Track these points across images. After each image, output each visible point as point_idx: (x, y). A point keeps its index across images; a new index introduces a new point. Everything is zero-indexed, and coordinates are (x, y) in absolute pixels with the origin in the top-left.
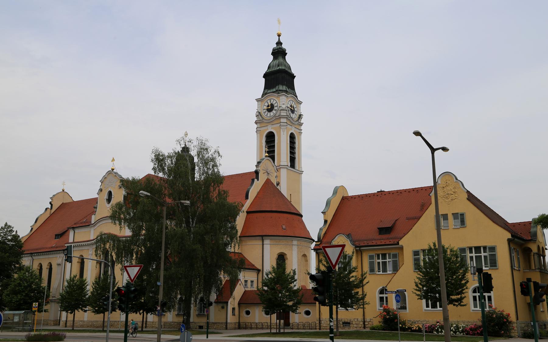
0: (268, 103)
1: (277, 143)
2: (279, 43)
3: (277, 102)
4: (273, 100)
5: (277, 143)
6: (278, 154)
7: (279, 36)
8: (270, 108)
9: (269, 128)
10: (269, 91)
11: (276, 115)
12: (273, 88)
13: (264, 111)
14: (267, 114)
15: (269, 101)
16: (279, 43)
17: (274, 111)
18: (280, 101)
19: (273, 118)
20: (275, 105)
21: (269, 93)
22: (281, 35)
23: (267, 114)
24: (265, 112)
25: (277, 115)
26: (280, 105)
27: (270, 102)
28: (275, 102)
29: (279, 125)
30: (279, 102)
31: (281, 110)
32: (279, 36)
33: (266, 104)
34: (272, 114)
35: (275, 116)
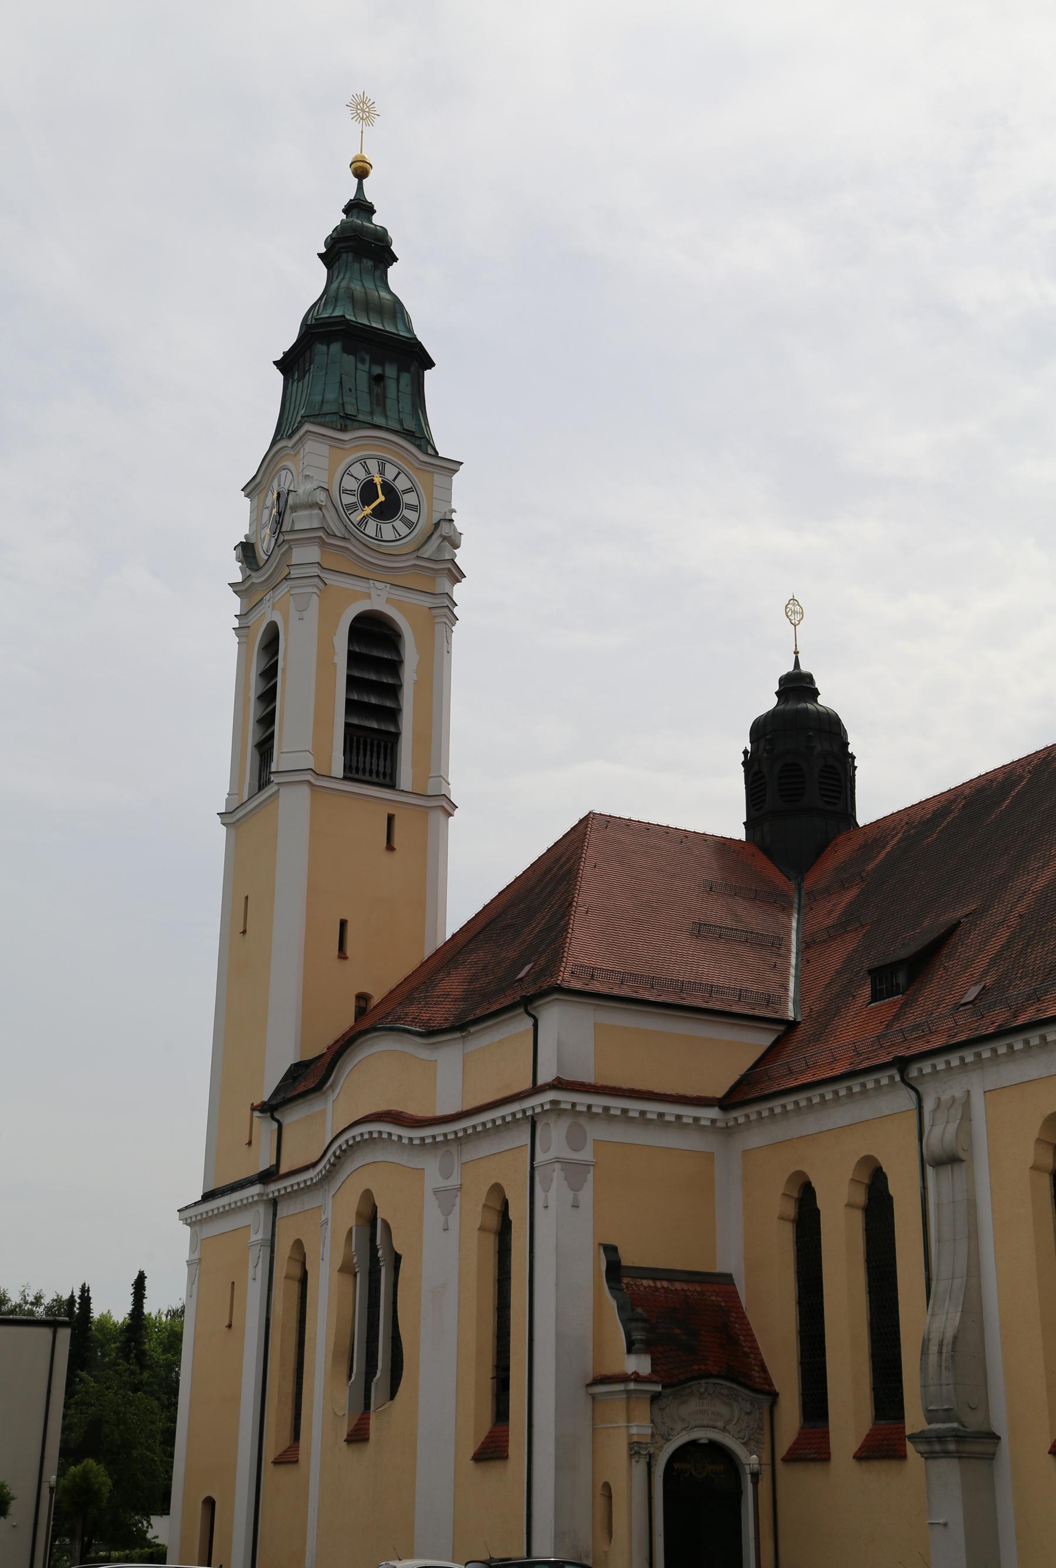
2: (359, 207)
4: (396, 471)
7: (361, 172)
16: (359, 207)
17: (398, 524)
19: (404, 558)
20: (408, 499)
22: (372, 173)
28: (401, 484)
32: (361, 172)
34: (387, 530)
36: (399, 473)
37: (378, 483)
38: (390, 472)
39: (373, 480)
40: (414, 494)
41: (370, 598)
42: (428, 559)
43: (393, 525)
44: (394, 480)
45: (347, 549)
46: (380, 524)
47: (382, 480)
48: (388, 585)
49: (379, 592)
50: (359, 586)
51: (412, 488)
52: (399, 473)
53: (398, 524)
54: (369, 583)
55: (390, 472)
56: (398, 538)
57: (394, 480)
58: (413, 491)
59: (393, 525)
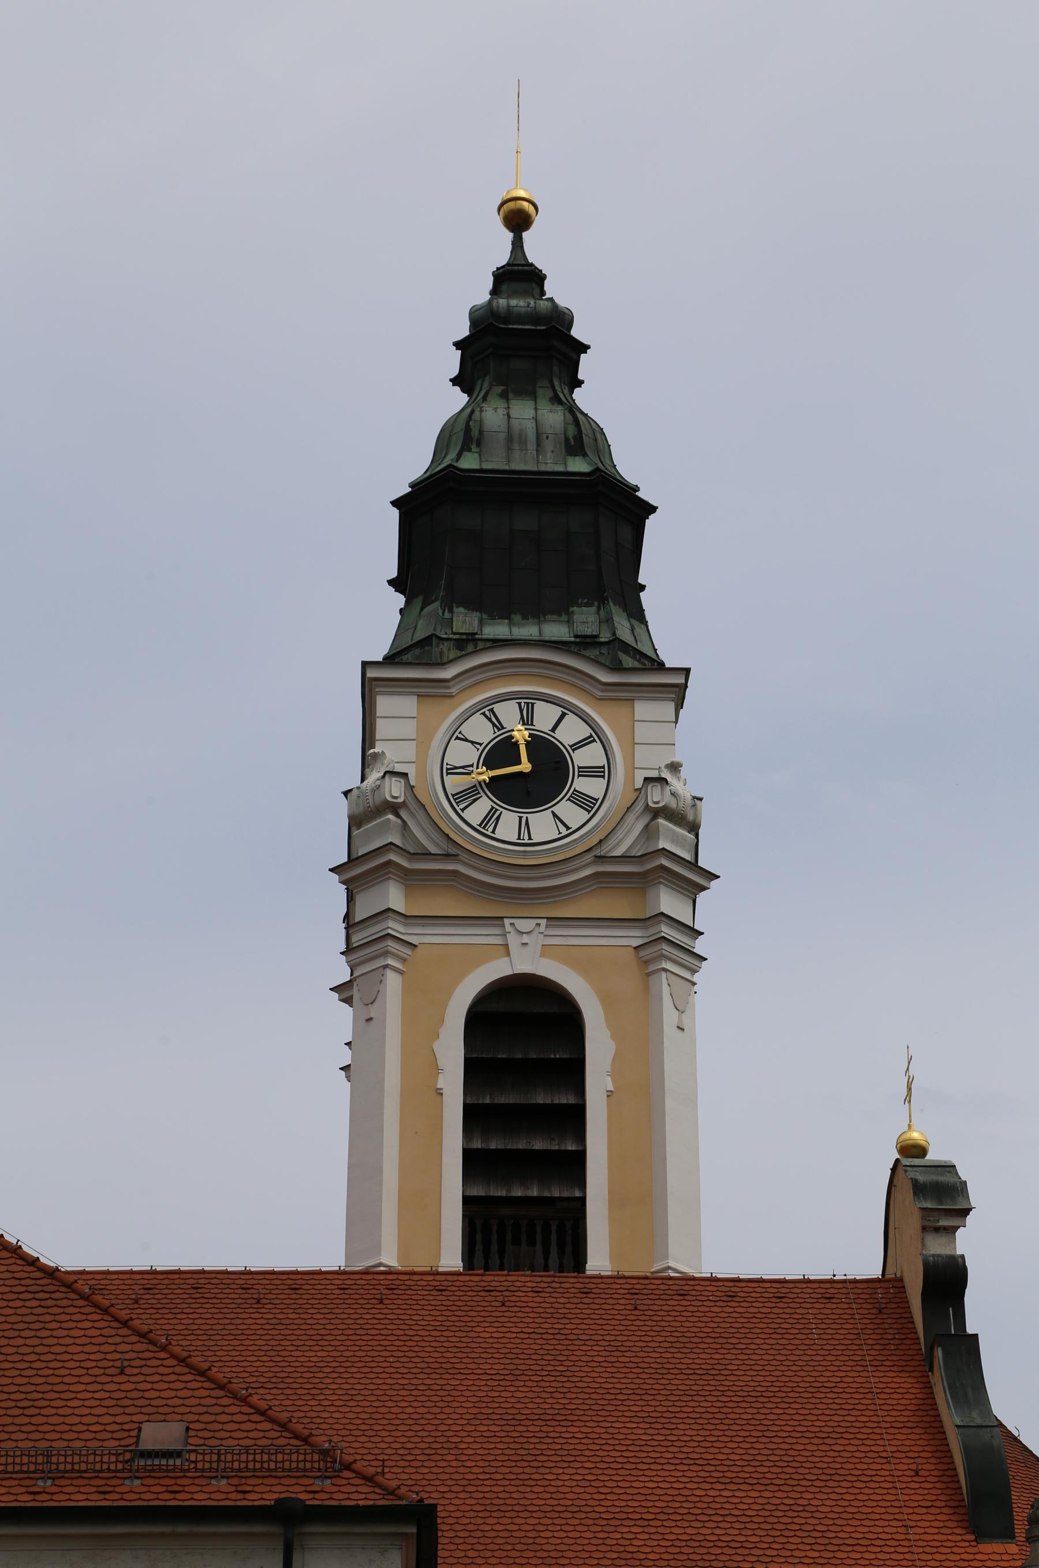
0: (498, 726)
1: (610, 1094)
3: (596, 736)
5: (610, 1094)
6: (616, 1200)
8: (525, 766)
9: (513, 940)
10: (498, 630)
11: (612, 842)
12: (536, 612)
13: (455, 783)
14: (491, 818)
15: (509, 713)
17: (566, 809)
18: (642, 732)
19: (577, 863)
21: (498, 643)
23: (491, 818)
24: (470, 794)
25: (625, 843)
26: (631, 768)
27: (527, 720)
28: (570, 732)
29: (634, 937)
30: (631, 744)
31: (657, 813)
33: (482, 731)
35: (604, 851)
36: (563, 715)
37: (522, 742)
38: (545, 716)
39: (512, 737)
40: (597, 746)
41: (508, 954)
42: (624, 858)
43: (554, 815)
44: (553, 730)
45: (455, 872)
46: (525, 816)
47: (530, 735)
48: (543, 922)
49: (525, 939)
50: (483, 936)
51: (591, 736)
52: (563, 715)
53: (566, 809)
54: (503, 926)
55: (545, 716)
56: (564, 832)
57: (553, 730)
58: (594, 741)
59: (554, 815)
